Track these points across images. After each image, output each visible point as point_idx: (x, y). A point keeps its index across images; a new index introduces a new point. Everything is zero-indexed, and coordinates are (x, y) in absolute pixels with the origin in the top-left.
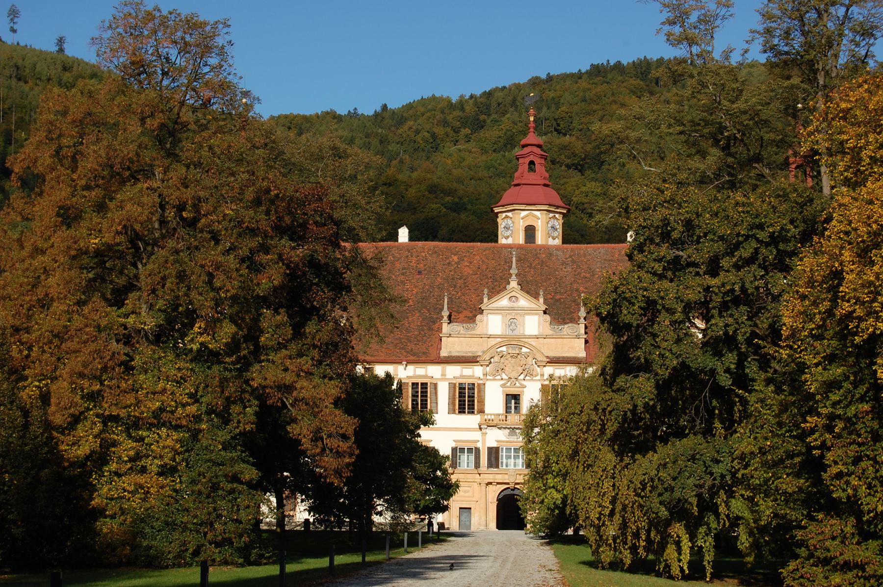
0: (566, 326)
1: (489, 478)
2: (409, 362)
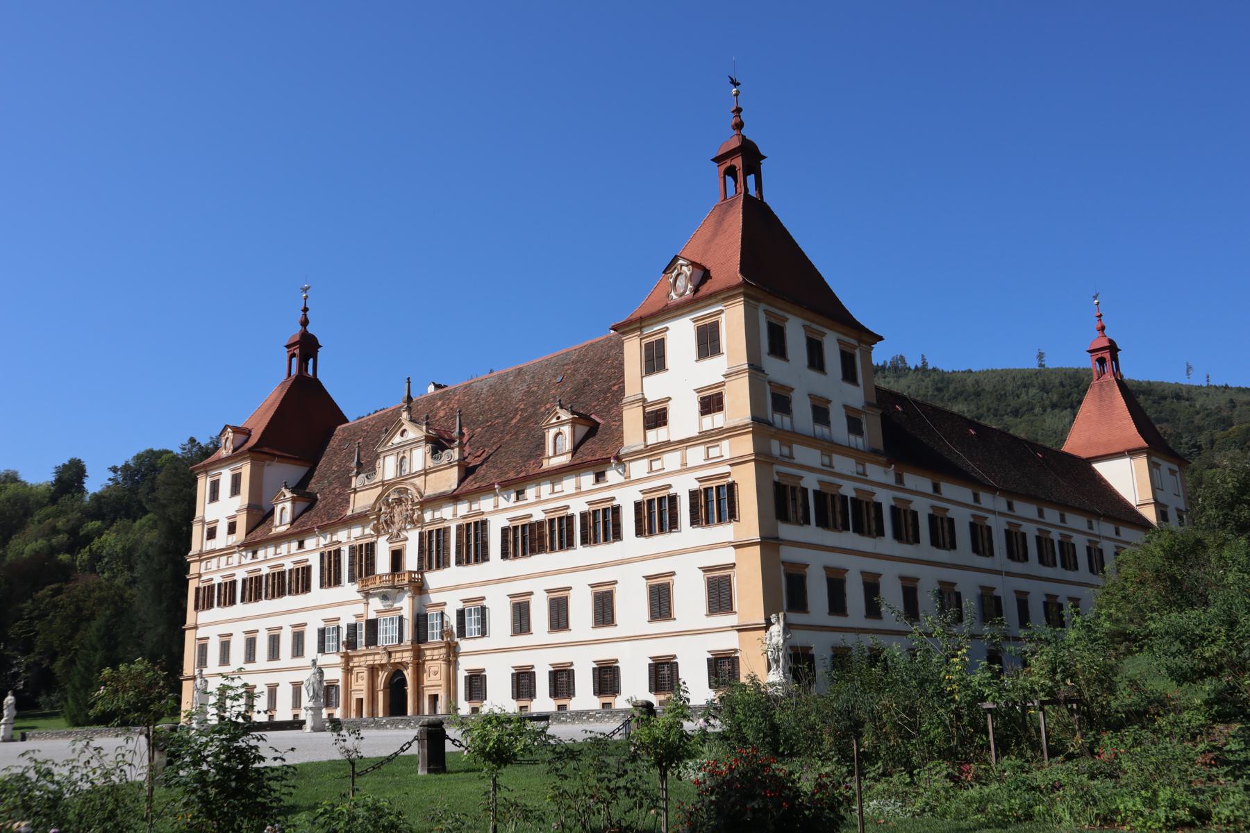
1: (370, 660)
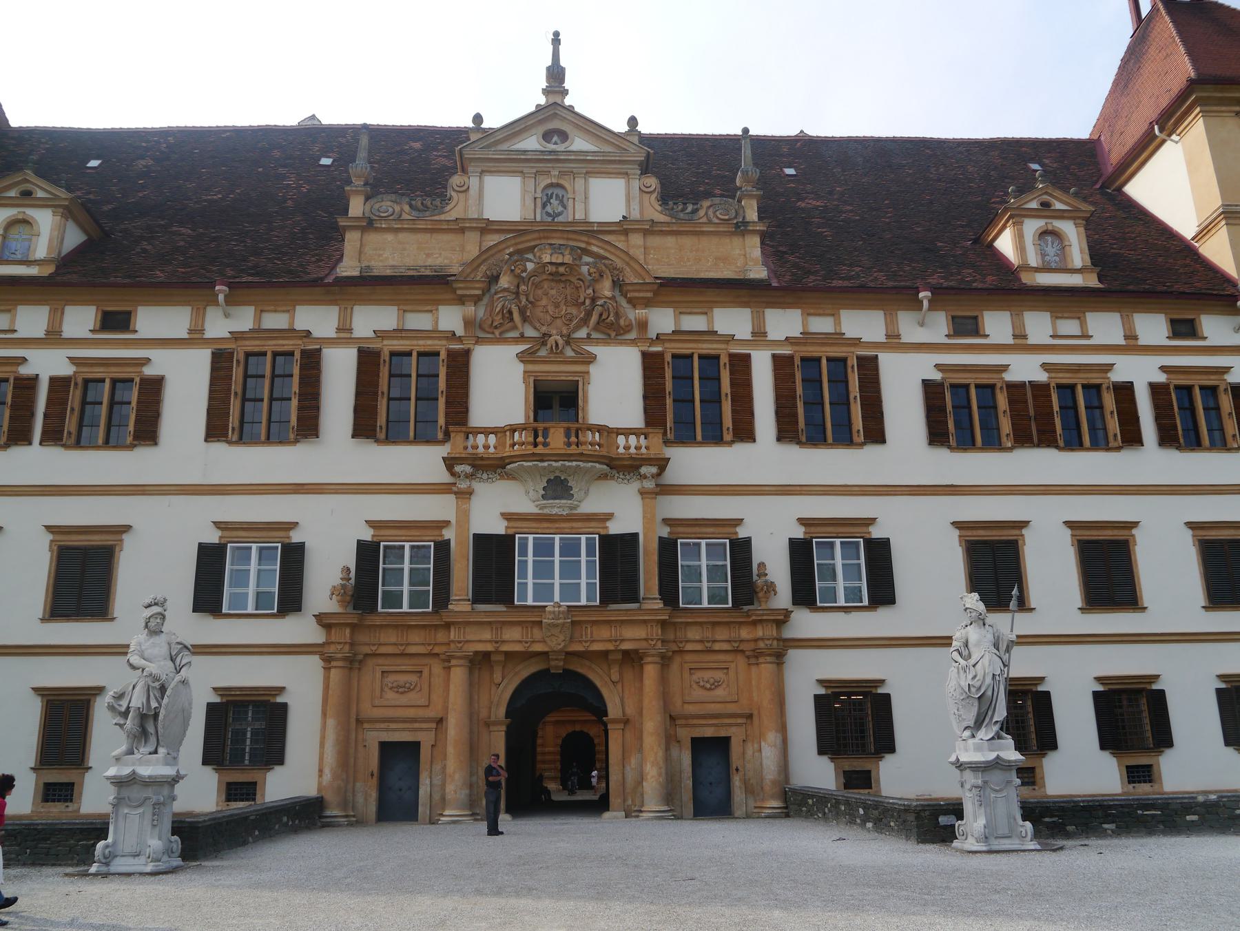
0: (706, 203)
1: (480, 640)
2: (239, 293)
